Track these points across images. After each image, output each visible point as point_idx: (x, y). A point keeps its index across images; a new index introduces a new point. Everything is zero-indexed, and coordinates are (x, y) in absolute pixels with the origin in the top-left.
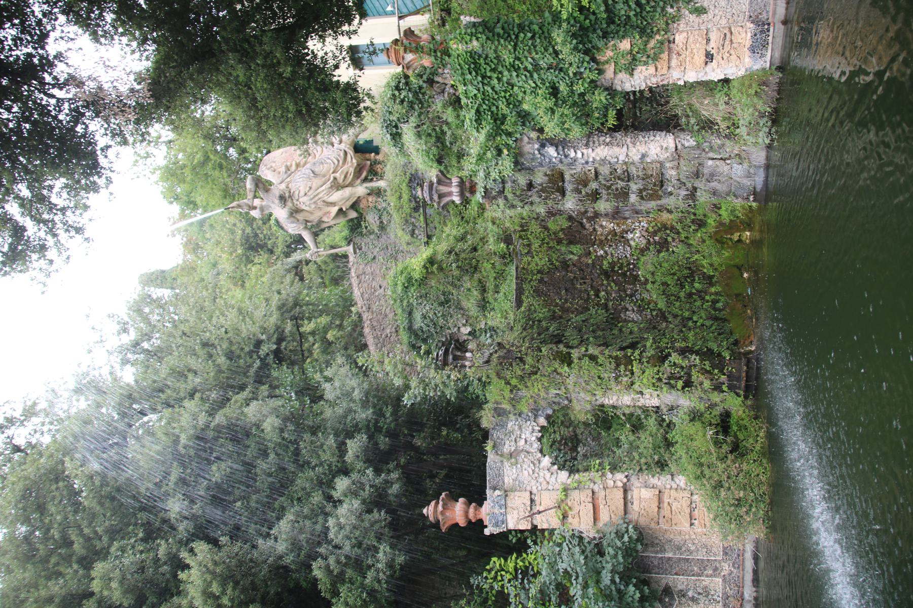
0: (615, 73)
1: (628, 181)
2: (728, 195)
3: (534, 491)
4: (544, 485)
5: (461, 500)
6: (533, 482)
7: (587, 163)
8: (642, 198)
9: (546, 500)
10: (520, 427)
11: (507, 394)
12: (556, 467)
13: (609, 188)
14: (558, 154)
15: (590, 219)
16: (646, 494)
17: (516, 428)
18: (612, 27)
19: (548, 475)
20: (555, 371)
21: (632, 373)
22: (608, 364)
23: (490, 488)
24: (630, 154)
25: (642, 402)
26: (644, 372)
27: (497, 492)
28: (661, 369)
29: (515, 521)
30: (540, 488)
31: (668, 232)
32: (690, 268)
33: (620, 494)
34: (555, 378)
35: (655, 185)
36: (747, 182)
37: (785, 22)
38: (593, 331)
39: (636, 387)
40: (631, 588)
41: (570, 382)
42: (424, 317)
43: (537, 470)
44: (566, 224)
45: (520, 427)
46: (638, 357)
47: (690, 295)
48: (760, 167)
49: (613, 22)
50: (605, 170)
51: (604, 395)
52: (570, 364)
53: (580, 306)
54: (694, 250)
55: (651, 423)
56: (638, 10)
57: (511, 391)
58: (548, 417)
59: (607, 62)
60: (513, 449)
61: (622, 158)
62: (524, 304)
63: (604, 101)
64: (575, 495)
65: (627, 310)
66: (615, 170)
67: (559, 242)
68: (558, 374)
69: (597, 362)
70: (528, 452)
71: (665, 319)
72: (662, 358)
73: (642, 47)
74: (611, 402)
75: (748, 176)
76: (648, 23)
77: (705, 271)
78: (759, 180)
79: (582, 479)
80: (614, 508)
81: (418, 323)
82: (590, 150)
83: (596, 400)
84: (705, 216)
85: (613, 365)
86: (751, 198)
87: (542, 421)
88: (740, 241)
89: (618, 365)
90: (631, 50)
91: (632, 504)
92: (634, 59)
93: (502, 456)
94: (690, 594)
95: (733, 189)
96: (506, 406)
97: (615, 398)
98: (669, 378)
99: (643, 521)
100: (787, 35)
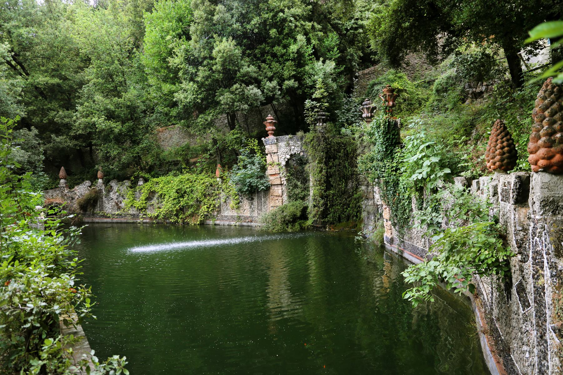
3: (278, 153)
5: (274, 128)
6: (281, 153)
9: (275, 158)
10: (298, 146)
11: (308, 140)
16: (280, 192)
19: (284, 158)
29: (268, 148)
34: (314, 158)
40: (246, 188)
42: (378, 90)
45: (298, 146)
57: (309, 142)
64: (278, 168)
81: (376, 88)
94: (252, 206)
99: (271, 191)
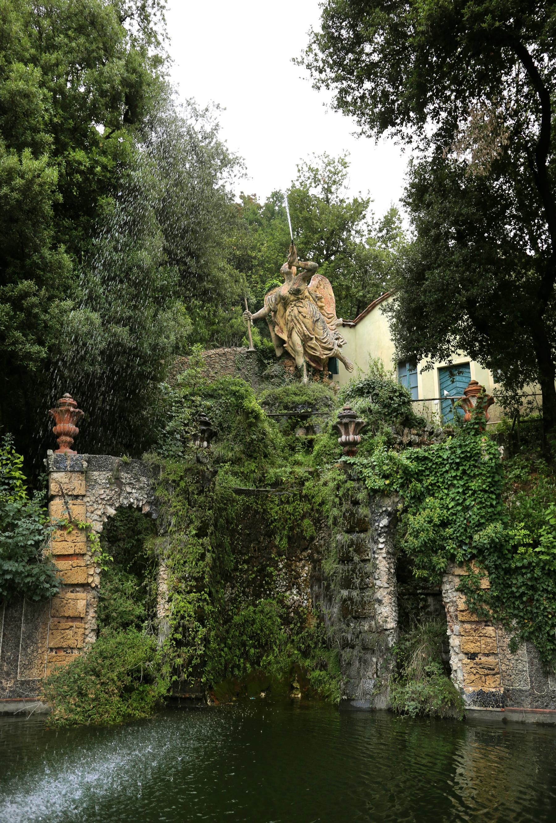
0: (459, 576)
1: (360, 589)
2: (348, 676)
4: (91, 509)
7: (374, 553)
8: (345, 600)
12: (106, 520)
13: (354, 571)
14: (382, 528)
15: (311, 557)
17: (142, 485)
18: (502, 573)
20: (191, 522)
21: (189, 592)
22: (198, 570)
23: (90, 458)
24: (381, 590)
25: (161, 601)
26: (190, 603)
27: (85, 464)
28: (192, 619)
30: (88, 504)
31: (299, 625)
32: (266, 644)
33: (81, 580)
35: (356, 611)
36: (358, 693)
37: (505, 721)
38: (219, 558)
39: (176, 596)
41: (182, 536)
43: (104, 502)
44: (307, 535)
46: (203, 598)
47: (244, 645)
48: (372, 704)
49: (506, 574)
50: (368, 568)
51: (167, 566)
52: (198, 536)
53: (235, 546)
54: (283, 648)
55: (140, 610)
56: (517, 594)
58: (148, 515)
59: (469, 569)
60: (124, 481)
61: (378, 583)
62: (237, 497)
63: (439, 566)
65: (233, 588)
66: (368, 577)
67: (291, 529)
68: (188, 525)
69: (198, 560)
70: (119, 495)
71: (225, 623)
72: (201, 618)
73: (484, 598)
74: (162, 573)
75: (365, 693)
76: (503, 603)
77: (264, 658)
78: (362, 704)
79: (95, 544)
80: (69, 574)
82: (385, 555)
83: (163, 559)
84: (313, 657)
85: (196, 575)
86: (345, 697)
87: (147, 509)
88: (292, 688)
89: (196, 579)
90: (480, 589)
91: (72, 592)
92: (472, 592)
93: (118, 470)
95: (352, 681)
96: (161, 476)
97: (165, 576)
98: (184, 626)
100: (491, 724)
